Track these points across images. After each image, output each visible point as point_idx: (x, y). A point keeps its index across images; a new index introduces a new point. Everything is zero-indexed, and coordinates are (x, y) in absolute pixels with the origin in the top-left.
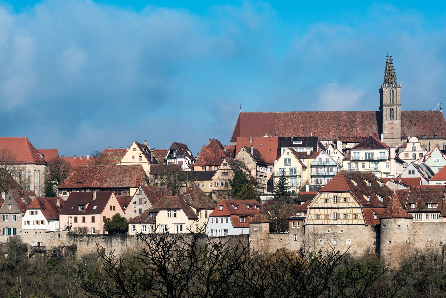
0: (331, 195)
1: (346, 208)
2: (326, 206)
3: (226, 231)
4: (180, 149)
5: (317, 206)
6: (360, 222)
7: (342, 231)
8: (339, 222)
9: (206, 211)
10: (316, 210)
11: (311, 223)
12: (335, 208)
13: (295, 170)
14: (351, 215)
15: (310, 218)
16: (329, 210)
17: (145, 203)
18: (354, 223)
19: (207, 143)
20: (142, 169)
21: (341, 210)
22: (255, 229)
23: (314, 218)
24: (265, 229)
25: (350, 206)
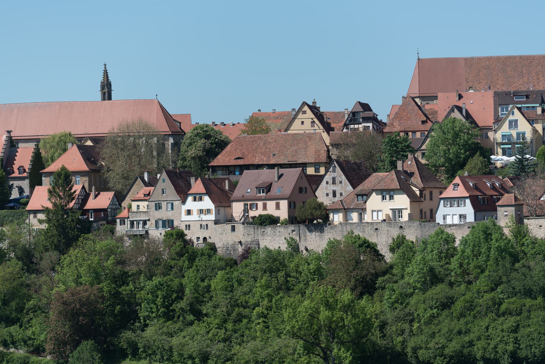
3: (462, 217)
4: (363, 112)
9: (431, 193)
13: (524, 134)
17: (341, 182)
19: (400, 103)
20: (322, 139)
22: (505, 213)
24: (519, 213)
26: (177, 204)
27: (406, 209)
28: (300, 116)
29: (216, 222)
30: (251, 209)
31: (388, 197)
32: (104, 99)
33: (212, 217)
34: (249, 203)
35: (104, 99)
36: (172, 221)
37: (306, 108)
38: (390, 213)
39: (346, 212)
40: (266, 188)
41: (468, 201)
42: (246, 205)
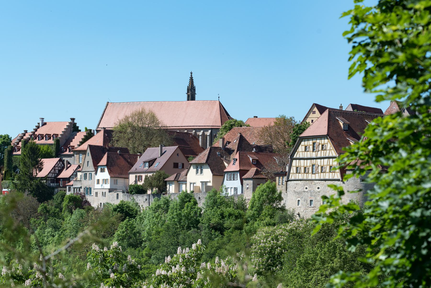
0: (311, 142)
1: (324, 158)
2: (306, 157)
5: (298, 156)
6: (336, 177)
7: (318, 188)
8: (317, 177)
10: (297, 161)
11: (293, 178)
12: (314, 159)
14: (328, 167)
15: (292, 172)
16: (309, 161)
18: (331, 178)
21: (319, 161)
22: (247, 186)
23: (295, 172)
25: (327, 155)
26: (93, 173)
27: (210, 182)
28: (311, 115)
29: (110, 190)
30: (139, 180)
31: (199, 170)
32: (188, 100)
33: (108, 186)
34: (138, 175)
35: (188, 100)
36: (91, 188)
37: (315, 109)
38: (200, 185)
39: (179, 184)
40: (149, 162)
41: (238, 174)
42: (136, 176)
